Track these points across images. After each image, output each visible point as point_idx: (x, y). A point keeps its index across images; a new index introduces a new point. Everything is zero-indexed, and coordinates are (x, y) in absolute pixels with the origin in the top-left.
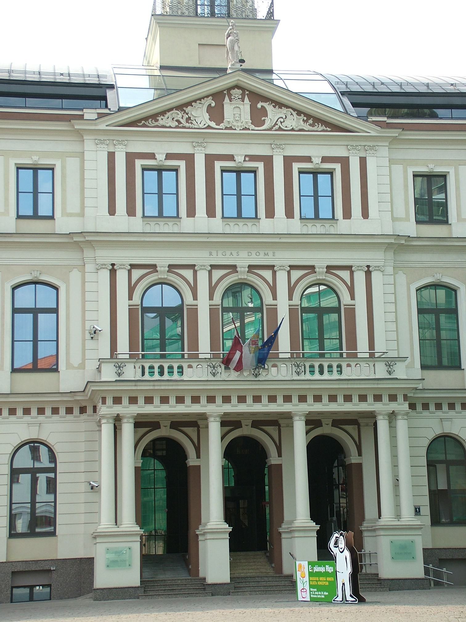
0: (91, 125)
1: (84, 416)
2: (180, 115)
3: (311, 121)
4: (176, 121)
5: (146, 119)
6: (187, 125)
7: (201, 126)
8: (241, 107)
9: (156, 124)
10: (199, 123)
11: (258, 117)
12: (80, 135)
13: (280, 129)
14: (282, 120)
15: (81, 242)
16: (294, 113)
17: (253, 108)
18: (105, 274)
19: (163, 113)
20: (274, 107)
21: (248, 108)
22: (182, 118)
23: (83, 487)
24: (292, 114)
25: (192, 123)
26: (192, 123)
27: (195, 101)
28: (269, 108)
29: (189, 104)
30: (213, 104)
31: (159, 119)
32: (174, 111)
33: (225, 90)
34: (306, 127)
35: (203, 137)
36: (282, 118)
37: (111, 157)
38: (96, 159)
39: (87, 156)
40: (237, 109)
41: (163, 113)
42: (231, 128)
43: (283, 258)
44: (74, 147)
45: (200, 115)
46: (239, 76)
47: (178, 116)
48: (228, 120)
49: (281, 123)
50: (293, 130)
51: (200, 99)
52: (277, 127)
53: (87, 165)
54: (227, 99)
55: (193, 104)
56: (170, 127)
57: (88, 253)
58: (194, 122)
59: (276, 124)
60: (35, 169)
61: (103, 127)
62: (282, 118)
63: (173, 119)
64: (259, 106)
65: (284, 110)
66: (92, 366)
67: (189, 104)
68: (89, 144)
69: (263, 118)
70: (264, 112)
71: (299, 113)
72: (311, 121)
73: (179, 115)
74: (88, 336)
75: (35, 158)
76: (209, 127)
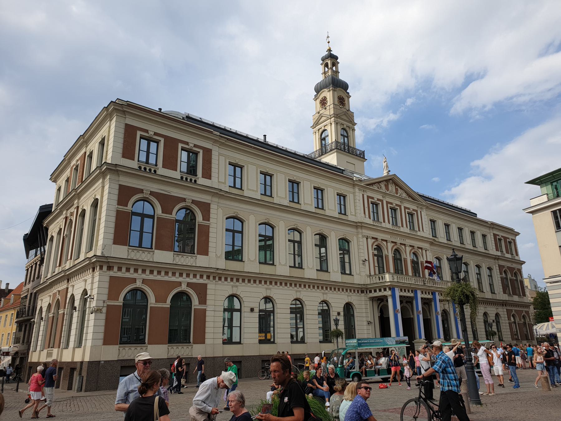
1: (363, 294)
11: (397, 190)
15: (358, 225)
18: (365, 239)
23: (365, 323)
28: (399, 189)
29: (380, 182)
37: (363, 195)
39: (357, 194)
43: (408, 242)
44: (351, 190)
53: (357, 197)
57: (360, 230)
61: (362, 184)
66: (363, 274)
68: (357, 190)
74: (362, 262)
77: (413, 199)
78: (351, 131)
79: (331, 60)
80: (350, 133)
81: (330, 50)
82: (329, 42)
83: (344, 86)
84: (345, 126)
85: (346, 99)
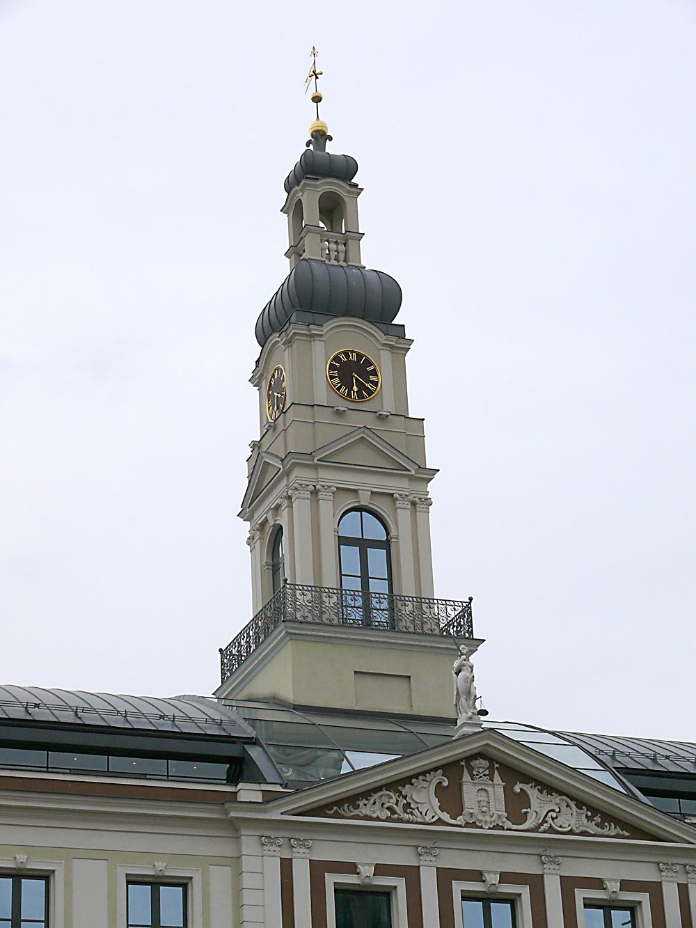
0: (259, 811)
2: (394, 800)
3: (598, 819)
4: (387, 808)
5: (340, 802)
6: (406, 816)
7: (427, 819)
8: (489, 789)
9: (356, 812)
10: (424, 814)
11: (516, 807)
12: (233, 828)
13: (551, 830)
14: (554, 815)
16: (572, 804)
17: (508, 791)
19: (366, 794)
20: (541, 791)
21: (500, 791)
22: (397, 804)
24: (568, 806)
25: (412, 813)
26: (412, 813)
27: (416, 776)
28: (533, 793)
29: (407, 780)
30: (446, 784)
31: (361, 804)
32: (385, 792)
33: (462, 760)
34: (592, 828)
35: (430, 839)
36: (553, 811)
37: (286, 867)
38: (261, 869)
39: (247, 864)
40: (482, 793)
41: (366, 794)
42: (474, 825)
44: (222, 848)
45: (425, 800)
46: (488, 739)
47: (391, 801)
48: (471, 811)
49: (553, 819)
50: (571, 832)
51: (424, 773)
52: (546, 826)
53: (247, 880)
54: (466, 777)
55: (413, 781)
56: (378, 819)
58: (416, 812)
59: (544, 821)
60: (156, 883)
61: (275, 815)
62: (553, 811)
63: (383, 804)
64: (517, 789)
65: (558, 799)
67: (407, 780)
68: (249, 844)
69: (524, 810)
70: (524, 800)
71: (580, 804)
72: (598, 819)
73: (392, 799)
75: (160, 865)
76: (440, 822)
77: (638, 831)
78: (404, 516)
79: (323, 184)
80: (402, 521)
81: (320, 137)
82: (317, 99)
83: (378, 304)
84: (365, 500)
85: (383, 363)
